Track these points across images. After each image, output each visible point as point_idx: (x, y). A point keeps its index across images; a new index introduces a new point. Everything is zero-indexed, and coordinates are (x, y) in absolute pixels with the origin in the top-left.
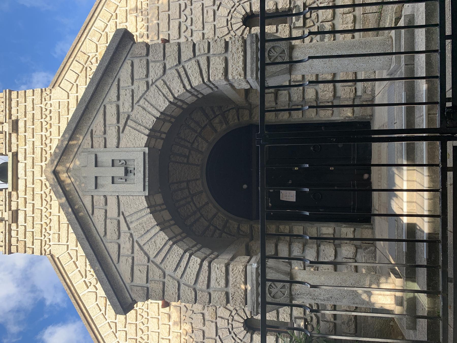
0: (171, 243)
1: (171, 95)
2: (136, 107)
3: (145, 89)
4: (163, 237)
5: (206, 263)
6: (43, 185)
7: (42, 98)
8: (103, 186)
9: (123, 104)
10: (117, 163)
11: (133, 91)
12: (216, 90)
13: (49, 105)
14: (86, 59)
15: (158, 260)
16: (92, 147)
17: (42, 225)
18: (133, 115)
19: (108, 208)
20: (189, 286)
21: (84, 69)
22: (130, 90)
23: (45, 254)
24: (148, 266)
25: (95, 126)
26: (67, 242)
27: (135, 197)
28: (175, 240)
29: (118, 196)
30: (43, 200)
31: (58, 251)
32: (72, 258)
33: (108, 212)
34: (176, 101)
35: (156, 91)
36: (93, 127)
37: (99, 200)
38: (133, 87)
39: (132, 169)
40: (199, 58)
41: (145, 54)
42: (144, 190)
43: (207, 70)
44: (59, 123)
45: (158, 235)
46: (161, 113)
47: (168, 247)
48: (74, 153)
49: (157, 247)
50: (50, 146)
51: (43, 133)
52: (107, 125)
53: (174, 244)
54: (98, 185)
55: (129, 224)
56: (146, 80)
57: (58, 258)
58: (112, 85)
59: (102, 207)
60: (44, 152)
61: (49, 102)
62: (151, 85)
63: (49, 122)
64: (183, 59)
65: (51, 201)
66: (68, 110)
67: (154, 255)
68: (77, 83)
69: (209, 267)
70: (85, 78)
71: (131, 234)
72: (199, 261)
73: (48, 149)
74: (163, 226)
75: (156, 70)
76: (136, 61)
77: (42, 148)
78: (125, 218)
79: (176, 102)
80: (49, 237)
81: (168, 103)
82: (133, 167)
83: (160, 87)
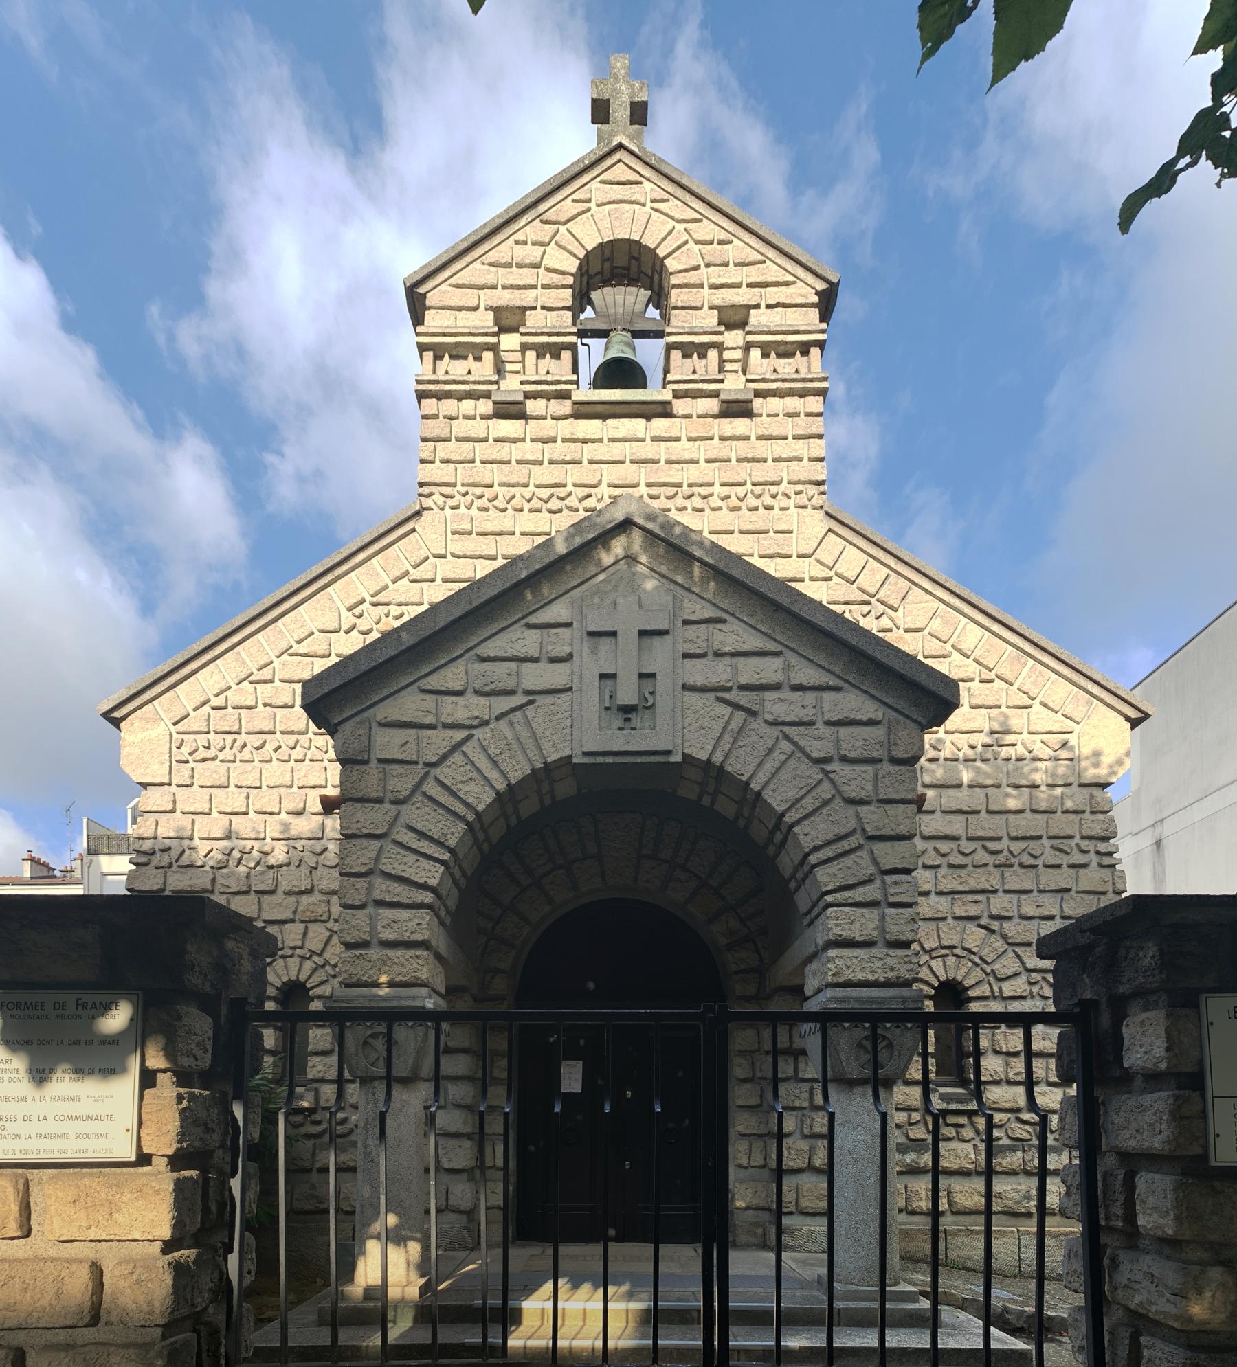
0: (471, 817)
1: (798, 816)
2: (775, 731)
3: (815, 755)
4: (482, 798)
5: (428, 897)
6: (587, 491)
7: (804, 483)
8: (594, 651)
9: (783, 700)
10: (648, 685)
11: (811, 723)
12: (806, 921)
13: (784, 502)
14: (891, 602)
15: (432, 789)
16: (686, 622)
17: (492, 486)
18: (757, 724)
19: (543, 665)
20: (377, 859)
21: (867, 598)
22: (814, 718)
23: (420, 495)
24: (416, 763)
25: (735, 628)
26: (453, 555)
27: (568, 730)
28: (477, 826)
29: (570, 689)
30: (552, 490)
31: (429, 532)
32: (415, 567)
33: (535, 665)
34: (784, 828)
35: (809, 781)
36: (732, 625)
37: (561, 642)
38: (820, 725)
39: (633, 724)
40: (878, 883)
41: (894, 753)
42: (586, 754)
43: (851, 901)
44: (741, 532)
45: (487, 788)
46: (759, 794)
47: (461, 809)
48: (671, 575)
49: (460, 786)
50: (685, 509)
51: (717, 489)
52: (734, 660)
53: (468, 824)
54: (596, 639)
55: (506, 719)
56: (836, 757)
57: (414, 530)
58: (828, 671)
59: (544, 650)
60: (670, 491)
61: (791, 503)
62: (823, 770)
63: (743, 505)
64: (880, 848)
65: (551, 512)
66: (770, 557)
67: (442, 778)
68: (835, 579)
69: (421, 906)
70: (846, 599)
71: (485, 723)
72: (433, 882)
73: (679, 501)
74: (507, 798)
75: (856, 780)
76: (879, 733)
77: (679, 485)
78: (520, 707)
79: (781, 829)
80: (462, 506)
81: (780, 808)
82: (638, 726)
83: (818, 790)
